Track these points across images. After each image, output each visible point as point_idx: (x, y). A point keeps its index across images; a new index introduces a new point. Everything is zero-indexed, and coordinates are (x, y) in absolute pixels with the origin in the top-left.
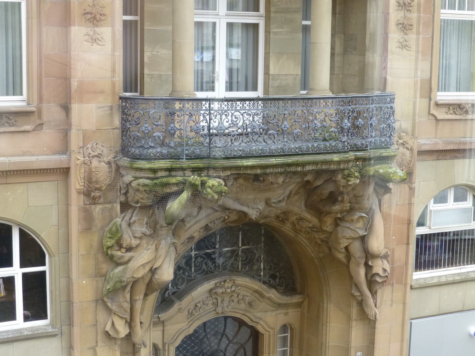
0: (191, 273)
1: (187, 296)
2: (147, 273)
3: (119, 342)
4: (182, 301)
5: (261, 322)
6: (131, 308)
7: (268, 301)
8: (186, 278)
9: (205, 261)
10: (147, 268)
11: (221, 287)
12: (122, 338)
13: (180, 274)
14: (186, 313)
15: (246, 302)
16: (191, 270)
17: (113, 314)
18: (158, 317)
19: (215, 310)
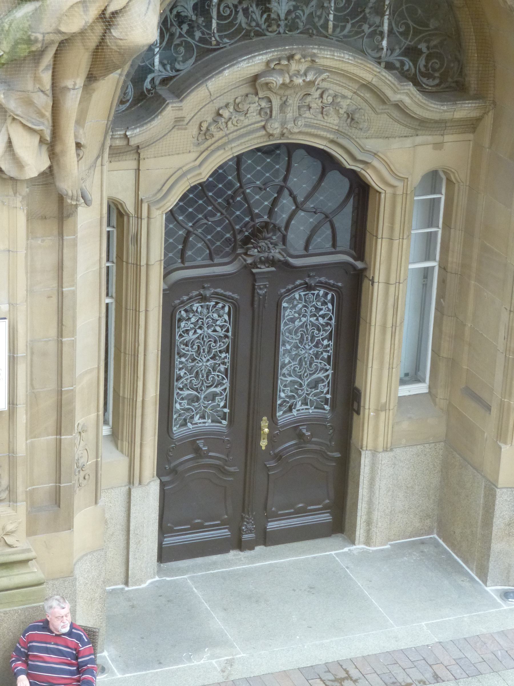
0: (208, 34)
1: (196, 87)
2: (94, 22)
3: (25, 190)
4: (185, 102)
5: (376, 163)
6: (53, 107)
7: (396, 114)
8: (196, 45)
9: (245, 6)
10: (93, 12)
11: (281, 72)
12: (32, 180)
13: (180, 33)
14: (195, 131)
15: (342, 111)
16: (209, 25)
17: (9, 120)
18: (126, 136)
19: (264, 127)
